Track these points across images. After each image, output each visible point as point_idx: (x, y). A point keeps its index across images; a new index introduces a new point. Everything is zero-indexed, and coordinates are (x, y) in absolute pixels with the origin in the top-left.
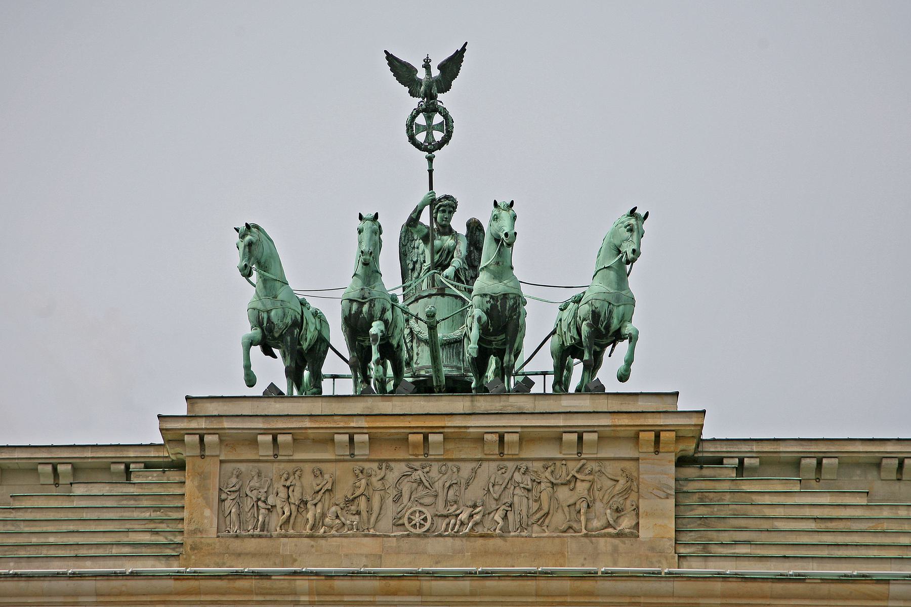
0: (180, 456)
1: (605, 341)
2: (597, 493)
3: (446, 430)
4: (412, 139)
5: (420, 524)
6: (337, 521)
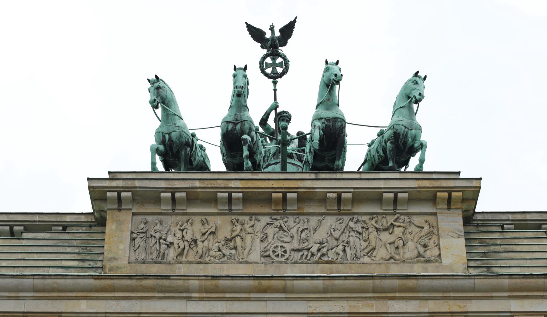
3: (299, 190)
4: (263, 71)
6: (219, 253)
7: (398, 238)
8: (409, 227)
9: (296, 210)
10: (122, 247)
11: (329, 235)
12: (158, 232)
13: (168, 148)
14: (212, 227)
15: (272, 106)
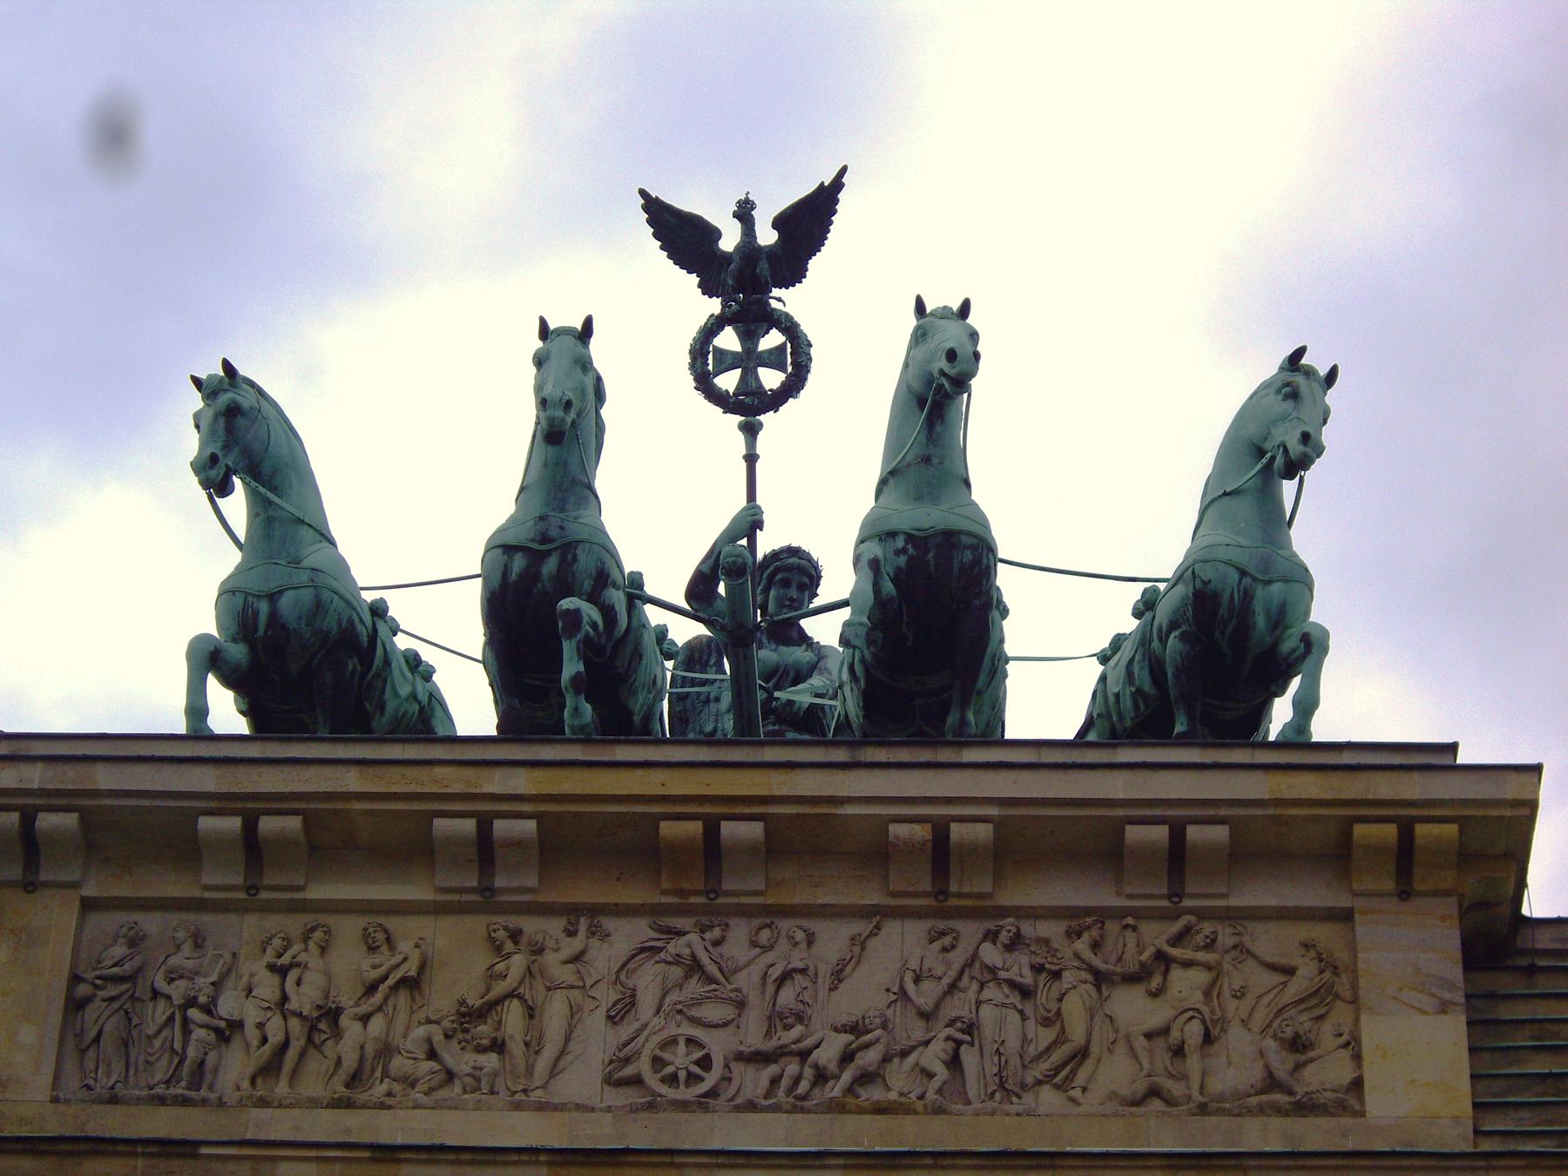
2: (1232, 1004)
4: (704, 384)
5: (690, 1074)
7: (1182, 1013)
8: (1235, 967)
11: (895, 997)
12: (181, 977)
14: (405, 959)
15: (736, 521)
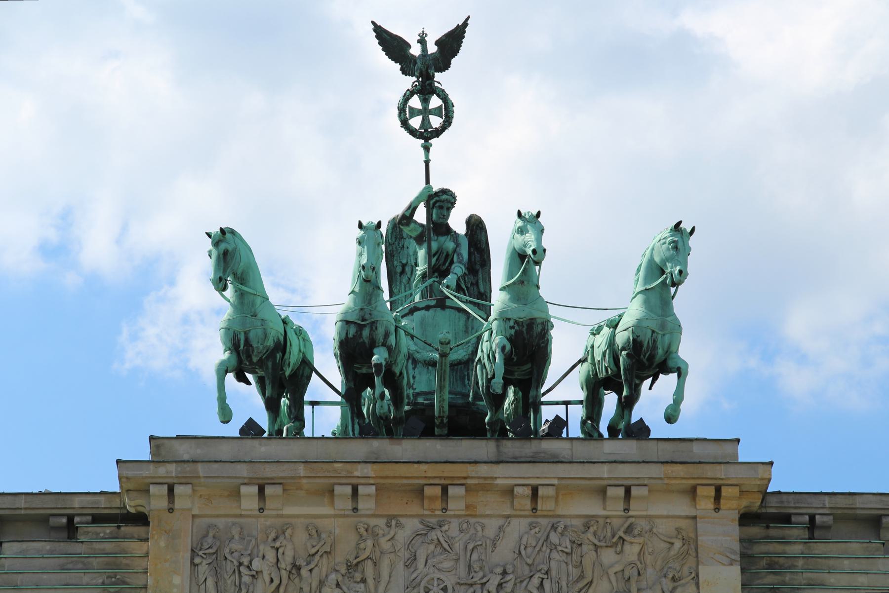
0: (141, 509)
1: (646, 373)
3: (469, 481)
4: (405, 124)
9: (463, 510)
10: (177, 580)
12: (236, 551)
13: (243, 357)
14: (325, 543)
